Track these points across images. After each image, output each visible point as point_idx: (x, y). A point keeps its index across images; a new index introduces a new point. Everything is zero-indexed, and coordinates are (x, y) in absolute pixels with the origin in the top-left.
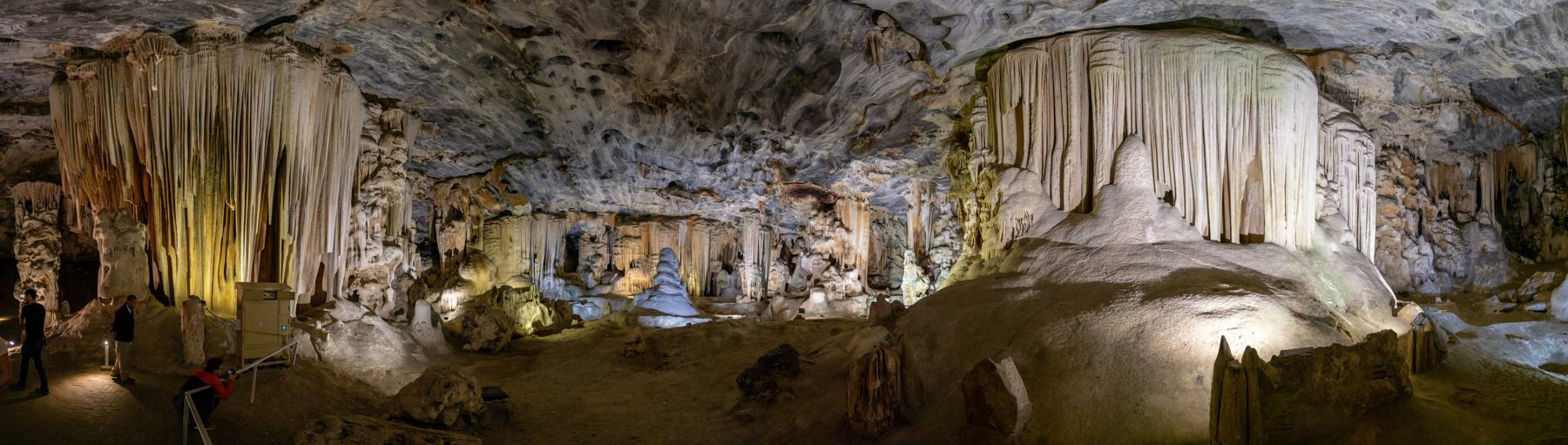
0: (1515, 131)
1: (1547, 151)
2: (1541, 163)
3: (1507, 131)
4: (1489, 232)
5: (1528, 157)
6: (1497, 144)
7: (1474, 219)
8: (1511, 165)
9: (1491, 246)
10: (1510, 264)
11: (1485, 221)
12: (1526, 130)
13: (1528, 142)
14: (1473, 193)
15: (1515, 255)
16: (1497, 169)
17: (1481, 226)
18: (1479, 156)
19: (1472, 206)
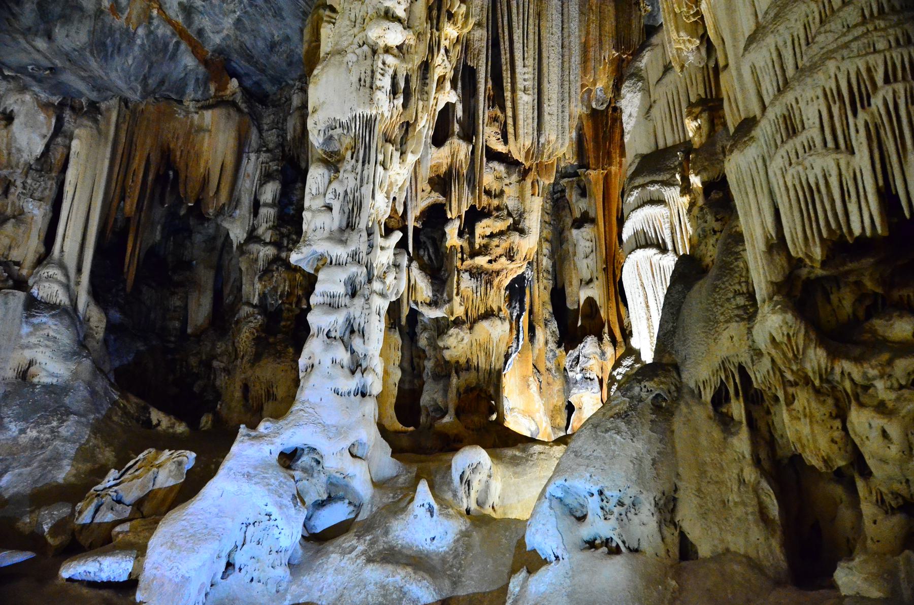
0: (188, 61)
1: (272, 138)
2: (252, 165)
3: (159, 50)
4: (51, 325)
5: (215, 139)
6: (121, 73)
7: (21, 284)
8: (167, 157)
9: (52, 368)
10: (97, 429)
11: (49, 288)
12: (218, 66)
13: (220, 103)
14: (37, 212)
15: (133, 403)
16: (122, 160)
17: (33, 305)
18: (76, 111)
19: (32, 245)
